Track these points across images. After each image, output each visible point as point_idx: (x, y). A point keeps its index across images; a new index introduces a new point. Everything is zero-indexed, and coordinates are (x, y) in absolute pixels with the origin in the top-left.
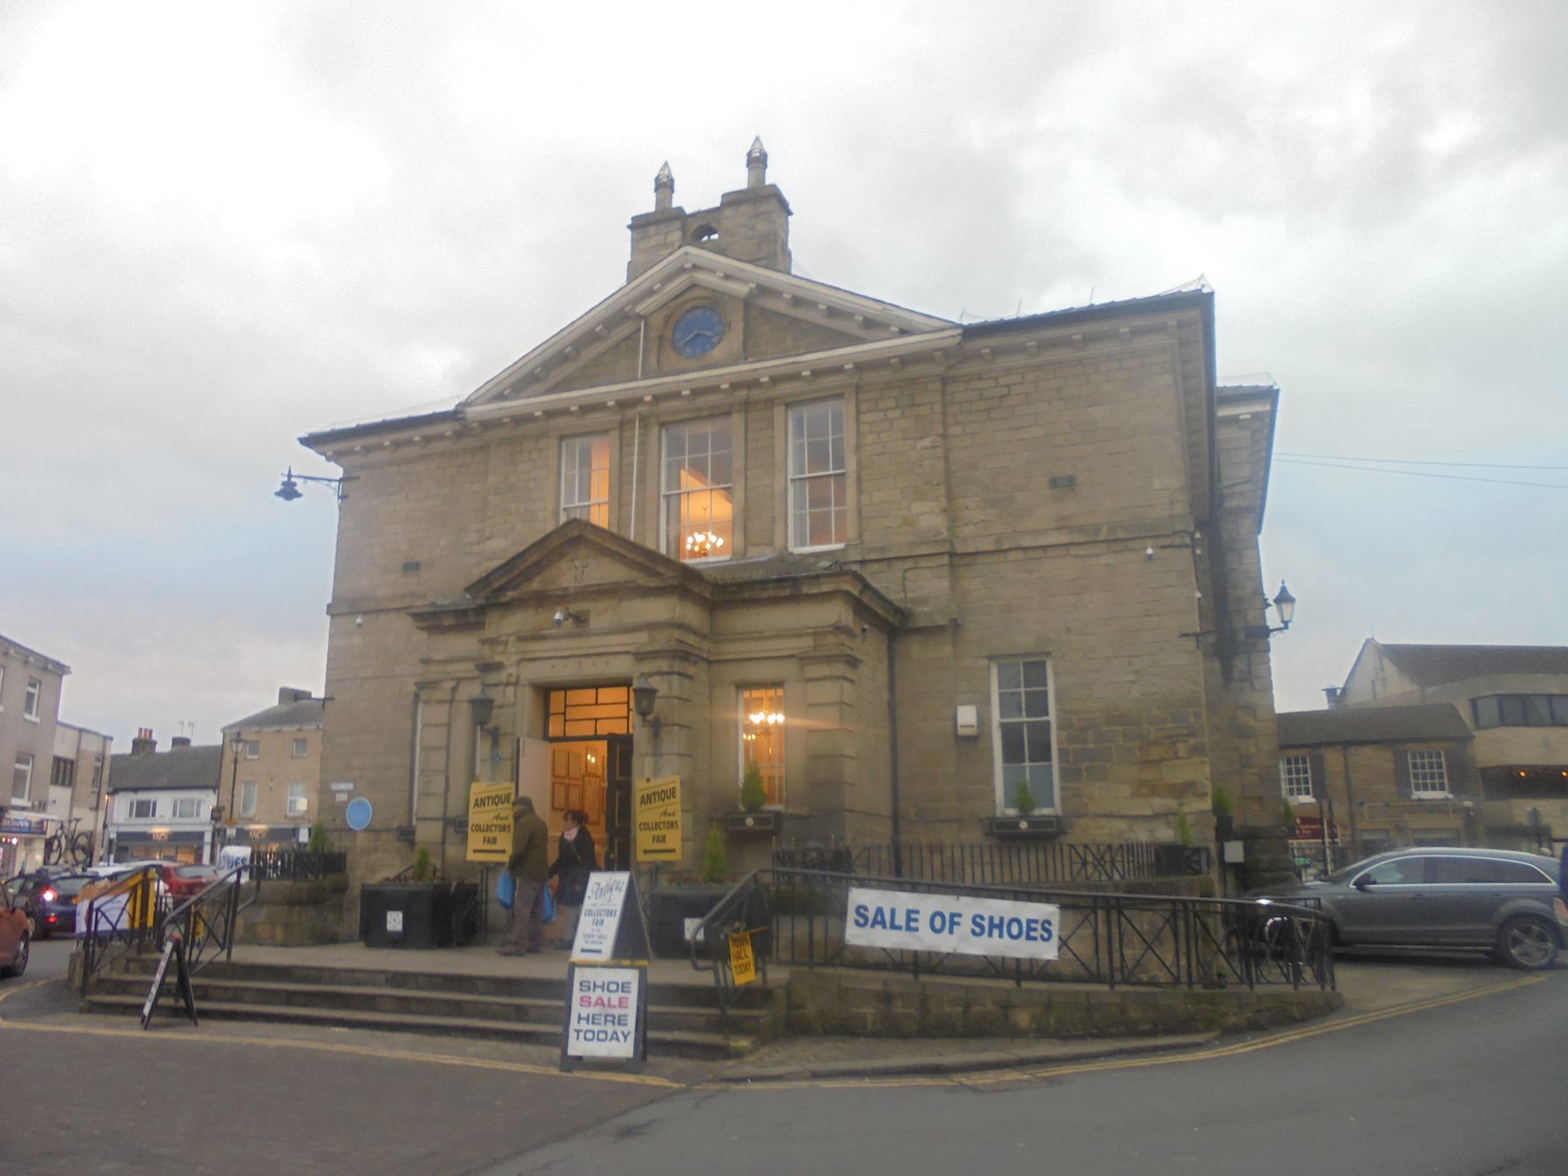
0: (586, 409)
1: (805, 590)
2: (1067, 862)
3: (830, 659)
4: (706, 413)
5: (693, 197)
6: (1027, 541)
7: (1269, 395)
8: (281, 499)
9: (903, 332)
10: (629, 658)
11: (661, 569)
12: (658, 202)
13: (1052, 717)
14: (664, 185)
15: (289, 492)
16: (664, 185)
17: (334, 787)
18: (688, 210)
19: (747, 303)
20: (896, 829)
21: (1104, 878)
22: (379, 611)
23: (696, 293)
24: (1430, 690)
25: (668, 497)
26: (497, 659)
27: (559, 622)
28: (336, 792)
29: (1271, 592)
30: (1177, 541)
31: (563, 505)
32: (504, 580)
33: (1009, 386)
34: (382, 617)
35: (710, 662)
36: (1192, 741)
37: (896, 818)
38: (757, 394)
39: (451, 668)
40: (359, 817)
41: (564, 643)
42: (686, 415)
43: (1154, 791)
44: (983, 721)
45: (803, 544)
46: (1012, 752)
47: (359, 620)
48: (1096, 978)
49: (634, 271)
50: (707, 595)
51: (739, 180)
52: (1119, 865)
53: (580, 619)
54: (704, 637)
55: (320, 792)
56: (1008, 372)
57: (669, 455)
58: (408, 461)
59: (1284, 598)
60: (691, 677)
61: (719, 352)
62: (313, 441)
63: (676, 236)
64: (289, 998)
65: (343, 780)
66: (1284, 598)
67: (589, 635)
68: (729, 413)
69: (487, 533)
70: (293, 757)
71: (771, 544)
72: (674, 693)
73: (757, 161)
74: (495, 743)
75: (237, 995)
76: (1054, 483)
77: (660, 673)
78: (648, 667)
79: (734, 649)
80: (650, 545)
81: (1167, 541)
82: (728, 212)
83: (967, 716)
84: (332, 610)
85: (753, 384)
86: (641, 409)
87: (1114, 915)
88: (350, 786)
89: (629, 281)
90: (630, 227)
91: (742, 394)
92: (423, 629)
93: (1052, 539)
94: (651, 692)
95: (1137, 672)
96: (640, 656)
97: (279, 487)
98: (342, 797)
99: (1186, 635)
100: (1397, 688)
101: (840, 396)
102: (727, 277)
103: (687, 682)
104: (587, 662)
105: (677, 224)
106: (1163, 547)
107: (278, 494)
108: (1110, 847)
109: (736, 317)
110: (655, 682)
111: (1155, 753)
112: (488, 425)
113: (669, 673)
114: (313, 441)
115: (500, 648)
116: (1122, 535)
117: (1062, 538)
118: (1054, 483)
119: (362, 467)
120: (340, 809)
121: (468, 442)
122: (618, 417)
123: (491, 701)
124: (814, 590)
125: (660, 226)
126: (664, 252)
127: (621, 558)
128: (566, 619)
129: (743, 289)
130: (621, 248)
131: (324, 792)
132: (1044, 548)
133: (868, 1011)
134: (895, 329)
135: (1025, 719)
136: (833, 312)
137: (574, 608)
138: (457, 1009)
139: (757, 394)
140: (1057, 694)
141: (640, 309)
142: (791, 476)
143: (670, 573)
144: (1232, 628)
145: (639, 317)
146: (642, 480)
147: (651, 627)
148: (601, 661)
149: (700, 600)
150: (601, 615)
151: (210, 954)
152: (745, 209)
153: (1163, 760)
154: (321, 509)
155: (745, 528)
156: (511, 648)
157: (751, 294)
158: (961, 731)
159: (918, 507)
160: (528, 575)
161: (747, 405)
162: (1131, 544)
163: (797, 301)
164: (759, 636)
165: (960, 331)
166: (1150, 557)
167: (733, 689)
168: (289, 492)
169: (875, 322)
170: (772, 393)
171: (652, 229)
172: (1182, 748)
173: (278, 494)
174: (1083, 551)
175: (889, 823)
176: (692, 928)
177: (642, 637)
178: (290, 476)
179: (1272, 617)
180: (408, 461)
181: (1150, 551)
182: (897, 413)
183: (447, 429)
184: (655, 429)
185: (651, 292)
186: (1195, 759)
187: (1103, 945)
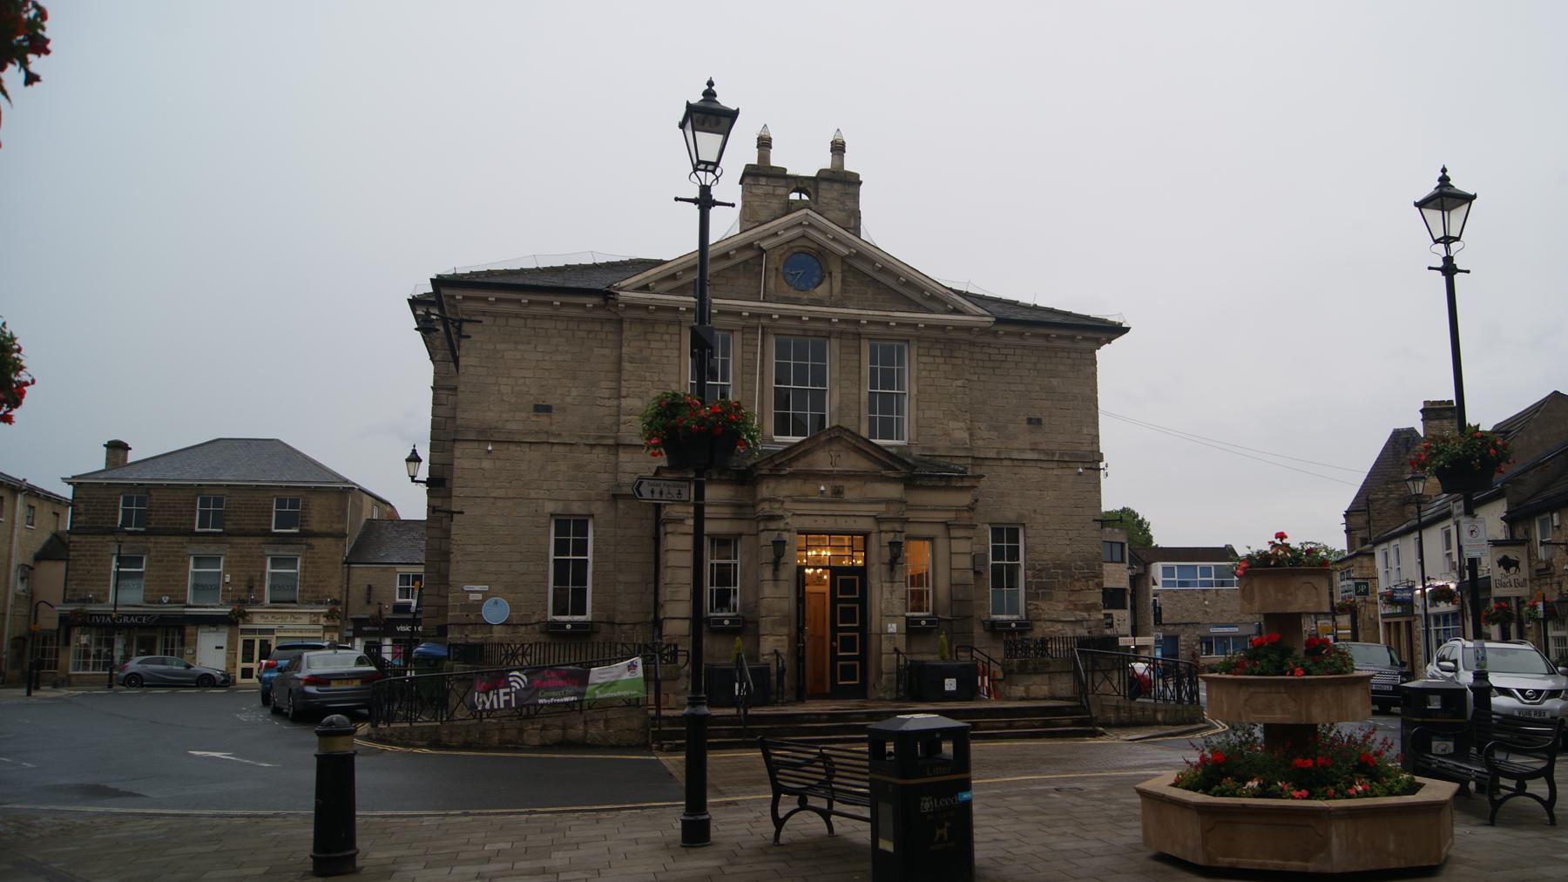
3: (966, 527)
6: (1015, 455)
9: (956, 311)
19: (843, 260)
26: (780, 513)
34: (512, 447)
38: (851, 328)
41: (827, 506)
46: (997, 583)
51: (826, 161)
53: (838, 492)
56: (1006, 346)
58: (535, 317)
61: (821, 291)
73: (838, 148)
76: (1030, 421)
78: (884, 527)
82: (824, 185)
86: (764, 321)
93: (1029, 455)
96: (878, 520)
102: (834, 239)
105: (783, 182)
117: (1035, 456)
118: (1030, 421)
121: (602, 314)
127: (867, 455)
136: (909, 284)
137: (839, 483)
139: (851, 328)
141: (764, 245)
146: (762, 373)
147: (888, 501)
150: (852, 491)
152: (837, 186)
156: (787, 505)
159: (952, 424)
160: (796, 458)
161: (841, 335)
164: (924, 508)
171: (763, 181)
174: (1045, 465)
177: (882, 507)
180: (535, 317)
183: (590, 302)
185: (776, 234)
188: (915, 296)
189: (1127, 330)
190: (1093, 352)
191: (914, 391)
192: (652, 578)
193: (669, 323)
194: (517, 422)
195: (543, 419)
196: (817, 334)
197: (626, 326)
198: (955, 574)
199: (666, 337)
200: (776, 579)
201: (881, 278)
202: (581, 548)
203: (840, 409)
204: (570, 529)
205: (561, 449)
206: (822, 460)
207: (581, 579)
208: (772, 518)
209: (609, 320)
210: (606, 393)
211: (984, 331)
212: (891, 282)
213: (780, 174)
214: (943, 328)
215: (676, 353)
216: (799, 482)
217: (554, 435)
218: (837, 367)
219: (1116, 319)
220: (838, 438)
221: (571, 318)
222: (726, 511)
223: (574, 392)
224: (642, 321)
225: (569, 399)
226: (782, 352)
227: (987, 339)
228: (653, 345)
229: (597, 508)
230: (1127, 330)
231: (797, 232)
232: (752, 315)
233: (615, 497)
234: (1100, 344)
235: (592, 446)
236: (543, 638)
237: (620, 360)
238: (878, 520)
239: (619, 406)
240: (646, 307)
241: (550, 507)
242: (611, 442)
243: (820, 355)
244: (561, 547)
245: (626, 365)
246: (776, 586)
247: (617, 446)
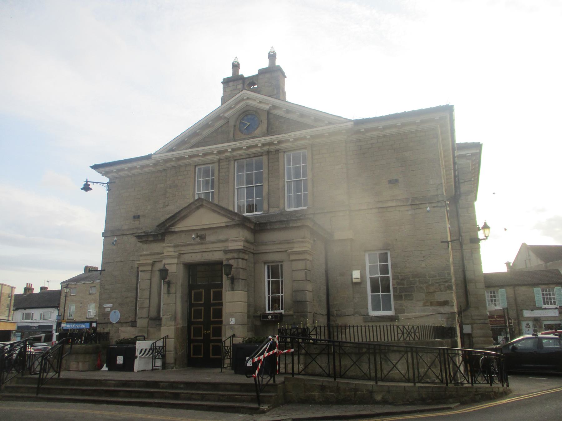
0: (205, 155)
1: (291, 225)
2: (396, 333)
4: (252, 156)
5: (247, 71)
7: (478, 146)
8: (84, 191)
9: (330, 123)
10: (222, 252)
11: (233, 217)
12: (234, 73)
13: (390, 275)
14: (236, 66)
15: (86, 188)
16: (236, 66)
17: (105, 306)
18: (245, 76)
19: (268, 113)
20: (329, 319)
21: (411, 339)
22: (123, 235)
24: (549, 264)
25: (238, 189)
27: (194, 239)
29: (480, 224)
30: (439, 205)
31: (196, 192)
32: (172, 222)
33: (372, 144)
34: (124, 237)
35: (254, 254)
36: (447, 284)
37: (329, 314)
38: (272, 148)
40: (115, 317)
42: (245, 157)
43: (432, 304)
44: (363, 276)
45: (289, 207)
46: (375, 289)
47: (115, 239)
48: (408, 381)
49: (224, 100)
50: (252, 227)
51: (265, 64)
52: (417, 334)
54: (251, 243)
55: (99, 308)
57: (238, 172)
59: (486, 227)
60: (246, 260)
61: (257, 132)
62: (95, 167)
63: (240, 86)
64: (83, 392)
65: (107, 303)
66: (486, 227)
67: (206, 243)
68: (262, 155)
69: (166, 204)
70: (90, 294)
71: (278, 207)
72: (240, 266)
73: (272, 56)
74: (169, 286)
75: (61, 391)
76: (390, 182)
77: (234, 258)
78: (230, 256)
79: (264, 248)
80: (231, 208)
81: (435, 205)
82: (261, 77)
83: (356, 275)
84: (104, 235)
85: (271, 144)
86: (226, 154)
87: (415, 355)
88: (111, 305)
89: (222, 104)
90: (222, 83)
91: (267, 148)
92: (140, 242)
93: (390, 204)
94: (230, 266)
95: (424, 257)
97: (83, 186)
98: (108, 310)
99: (442, 242)
100: (536, 263)
102: (260, 102)
103: (245, 261)
105: (241, 81)
106: (434, 207)
107: (82, 189)
108: (413, 327)
109: (264, 118)
110: (232, 262)
111: (432, 289)
112: (166, 161)
113: (237, 258)
114: (95, 167)
116: (418, 203)
117: (394, 204)
118: (390, 182)
119: (116, 178)
122: (217, 158)
123: (168, 270)
124: (295, 225)
125: (235, 82)
126: (236, 92)
128: (197, 237)
129: (267, 107)
130: (218, 91)
131: (101, 307)
132: (387, 207)
133: (316, 394)
134: (327, 122)
135: (379, 276)
136: (302, 115)
137: (200, 233)
138: (151, 395)
140: (392, 265)
142: (286, 180)
143: (236, 219)
144: (466, 239)
149: (249, 229)
151: (51, 374)
153: (435, 292)
154: (100, 195)
155: (268, 201)
157: (270, 109)
158: (354, 281)
162: (421, 206)
163: (288, 111)
165: (352, 123)
166: (428, 211)
167: (263, 264)
168: (86, 188)
171: (231, 84)
172: (442, 287)
173: (82, 189)
175: (326, 317)
176: (120, 360)
178: (87, 181)
179: (481, 235)
181: (428, 209)
184: (233, 162)
185: (230, 108)
186: (448, 291)
187: (411, 366)
195: (137, 222)
196: (256, 155)
199: (185, 173)
200: (169, 292)
203: (269, 194)
219: (443, 104)
220: (202, 206)
223: (149, 207)
224: (175, 167)
226: (240, 169)
243: (259, 166)
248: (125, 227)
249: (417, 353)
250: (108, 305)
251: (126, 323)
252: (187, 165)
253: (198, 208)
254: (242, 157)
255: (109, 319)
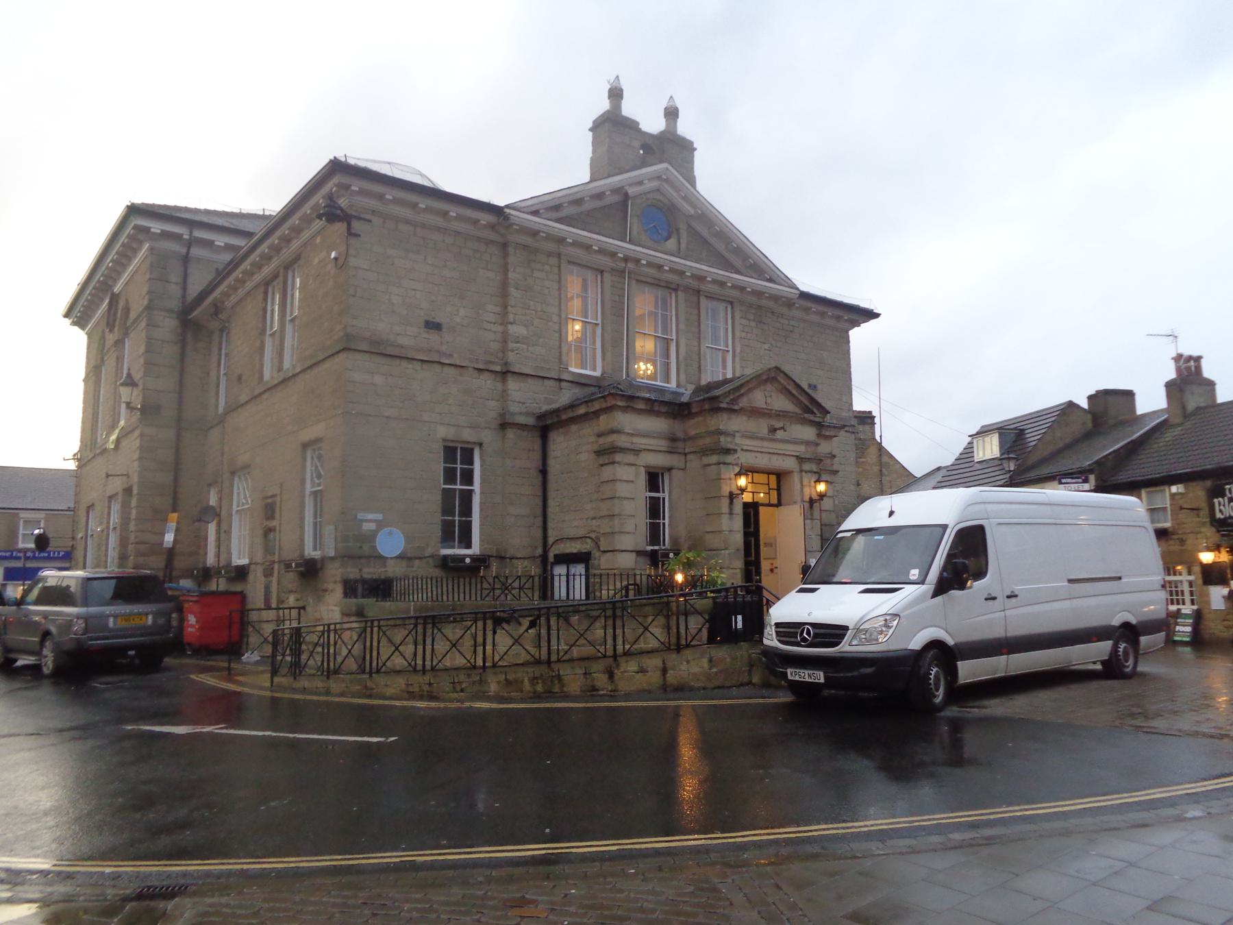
0: (601, 251)
9: (770, 280)
14: (616, 94)
16: (616, 94)
23: (659, 197)
26: (731, 446)
28: (362, 521)
34: (404, 363)
38: (694, 284)
39: (635, 440)
56: (793, 318)
61: (671, 244)
68: (676, 290)
69: (511, 320)
73: (672, 114)
78: (806, 467)
86: (630, 265)
88: (379, 516)
96: (800, 459)
98: (367, 527)
101: (731, 303)
104: (775, 458)
115: (729, 439)
119: (373, 212)
120: (371, 537)
141: (631, 191)
145: (626, 195)
147: (808, 443)
148: (780, 457)
156: (738, 440)
157: (691, 216)
169: (759, 266)
170: (702, 287)
180: (424, 226)
182: (753, 324)
183: (485, 218)
185: (641, 183)
188: (737, 262)
189: (877, 315)
190: (847, 332)
191: (738, 350)
192: (539, 511)
193: (550, 254)
194: (410, 337)
195: (433, 337)
197: (511, 250)
198: (824, 515)
199: (547, 268)
200: (731, 514)
201: (712, 240)
202: (468, 477)
204: (458, 458)
205: (451, 371)
206: (759, 398)
207: (467, 510)
208: (728, 451)
209: (492, 242)
210: (492, 318)
211: (789, 304)
212: (720, 247)
213: (630, 126)
214: (759, 294)
215: (556, 286)
216: (745, 418)
217: (444, 354)
218: (682, 317)
220: (774, 379)
221: (458, 233)
222: (662, 444)
223: (462, 312)
225: (458, 320)
227: (784, 310)
228: (536, 274)
229: (487, 436)
230: (877, 315)
231: (654, 184)
232: (626, 259)
233: (504, 426)
234: (856, 324)
235: (480, 370)
236: (437, 573)
237: (504, 284)
238: (800, 459)
239: (505, 333)
240: (534, 233)
241: (443, 432)
242: (498, 368)
244: (450, 476)
245: (512, 290)
246: (731, 519)
247: (505, 374)
248: (402, 341)
249: (434, 625)
250: (370, 516)
251: (420, 558)
252: (550, 254)
253: (766, 381)
254: (648, 280)
255: (374, 547)
